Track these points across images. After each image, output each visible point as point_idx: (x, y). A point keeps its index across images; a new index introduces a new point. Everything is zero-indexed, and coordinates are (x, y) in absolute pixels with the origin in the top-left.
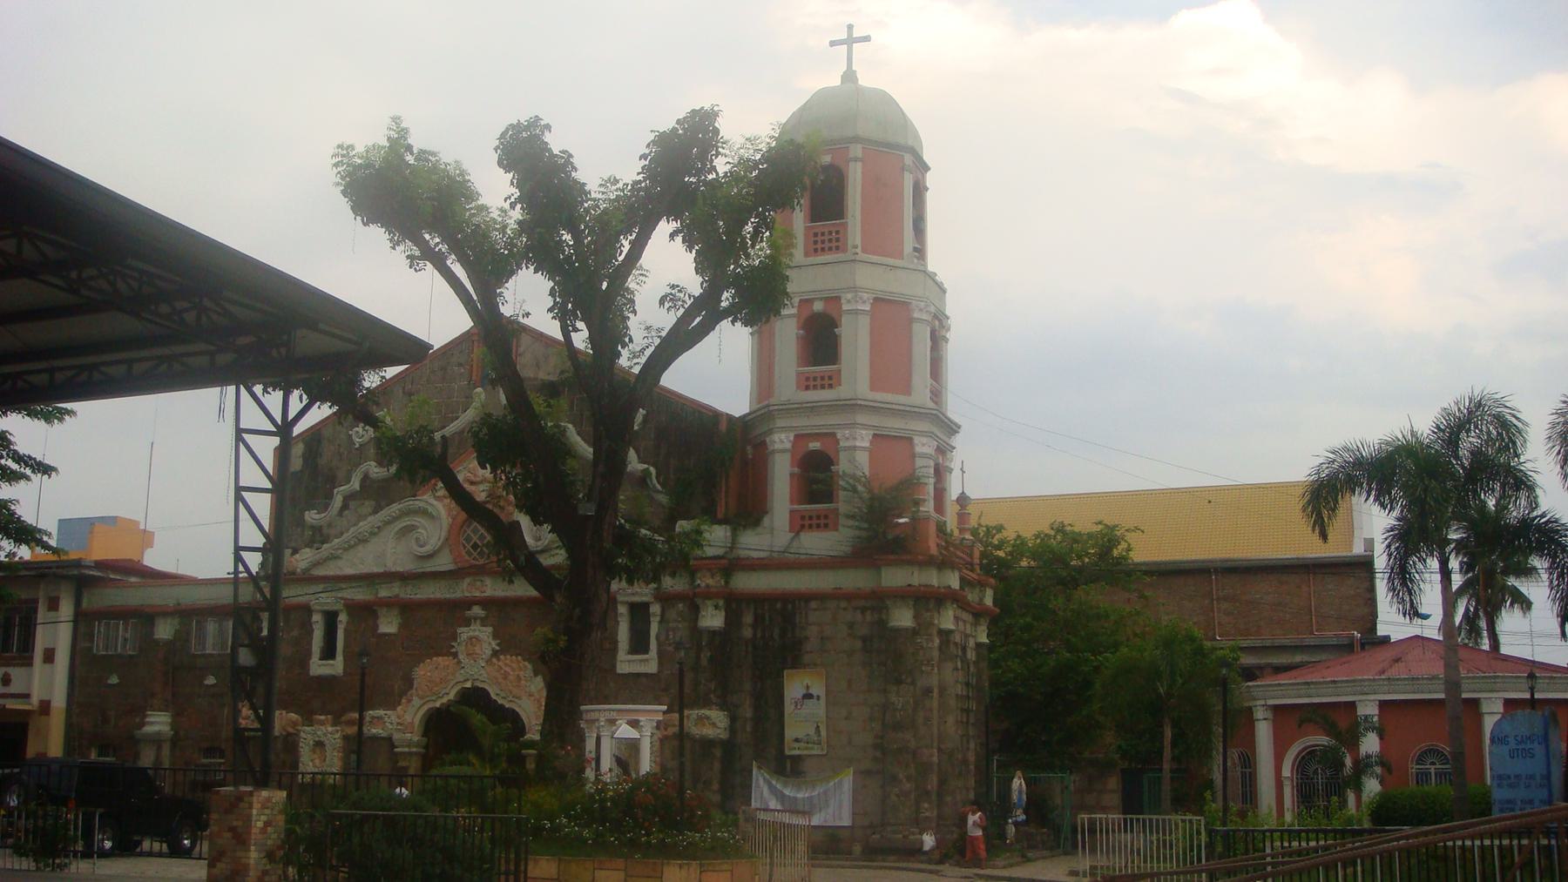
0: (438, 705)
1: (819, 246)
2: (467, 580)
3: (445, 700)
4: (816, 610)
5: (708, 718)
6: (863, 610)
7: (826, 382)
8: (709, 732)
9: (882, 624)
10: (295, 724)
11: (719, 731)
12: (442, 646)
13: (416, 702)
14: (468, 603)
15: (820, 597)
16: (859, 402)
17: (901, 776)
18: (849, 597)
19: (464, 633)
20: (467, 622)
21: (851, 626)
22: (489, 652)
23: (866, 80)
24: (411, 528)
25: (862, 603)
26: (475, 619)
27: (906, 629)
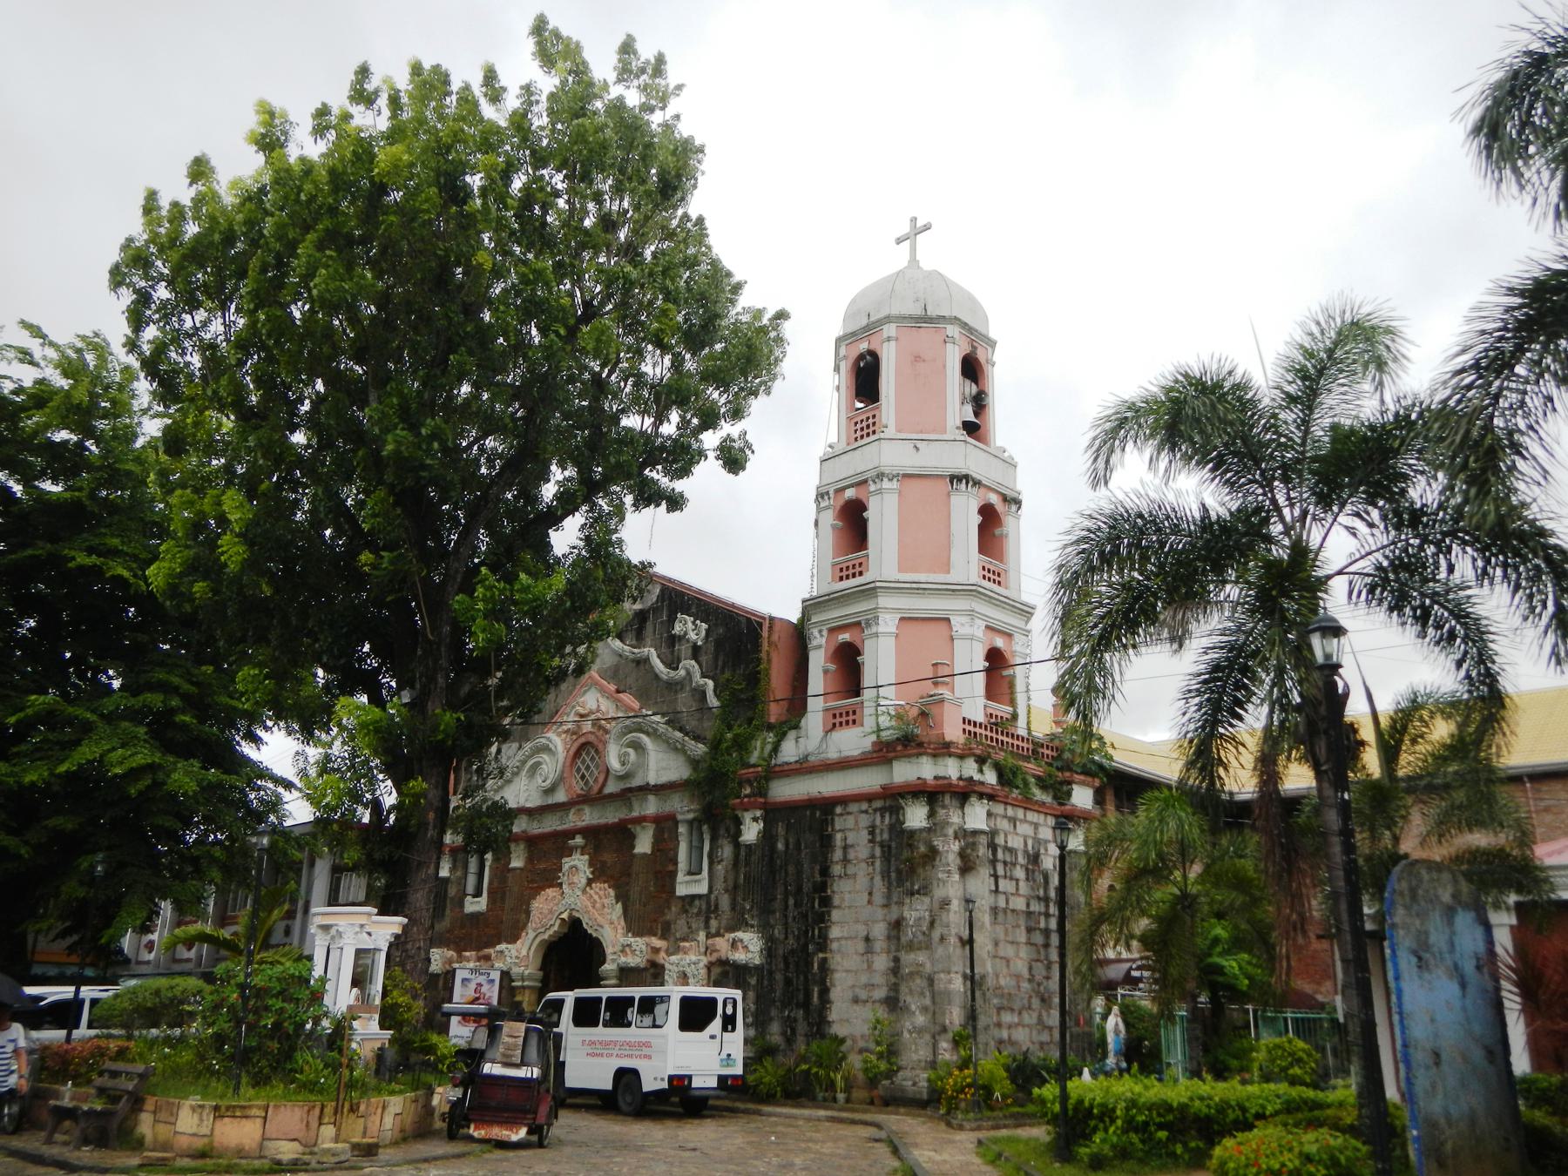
0: (546, 937)
1: (859, 433)
2: (573, 811)
3: (551, 932)
4: (841, 815)
5: (741, 941)
6: (882, 810)
7: (858, 569)
8: (740, 956)
9: (898, 829)
10: (450, 962)
11: (750, 955)
12: (550, 878)
13: (531, 934)
14: (571, 834)
15: (844, 800)
16: (878, 584)
17: (913, 1007)
18: (869, 798)
19: (567, 863)
20: (570, 852)
21: (872, 831)
22: (584, 881)
23: (926, 263)
24: (538, 764)
25: (878, 804)
26: (576, 848)
27: (921, 830)
